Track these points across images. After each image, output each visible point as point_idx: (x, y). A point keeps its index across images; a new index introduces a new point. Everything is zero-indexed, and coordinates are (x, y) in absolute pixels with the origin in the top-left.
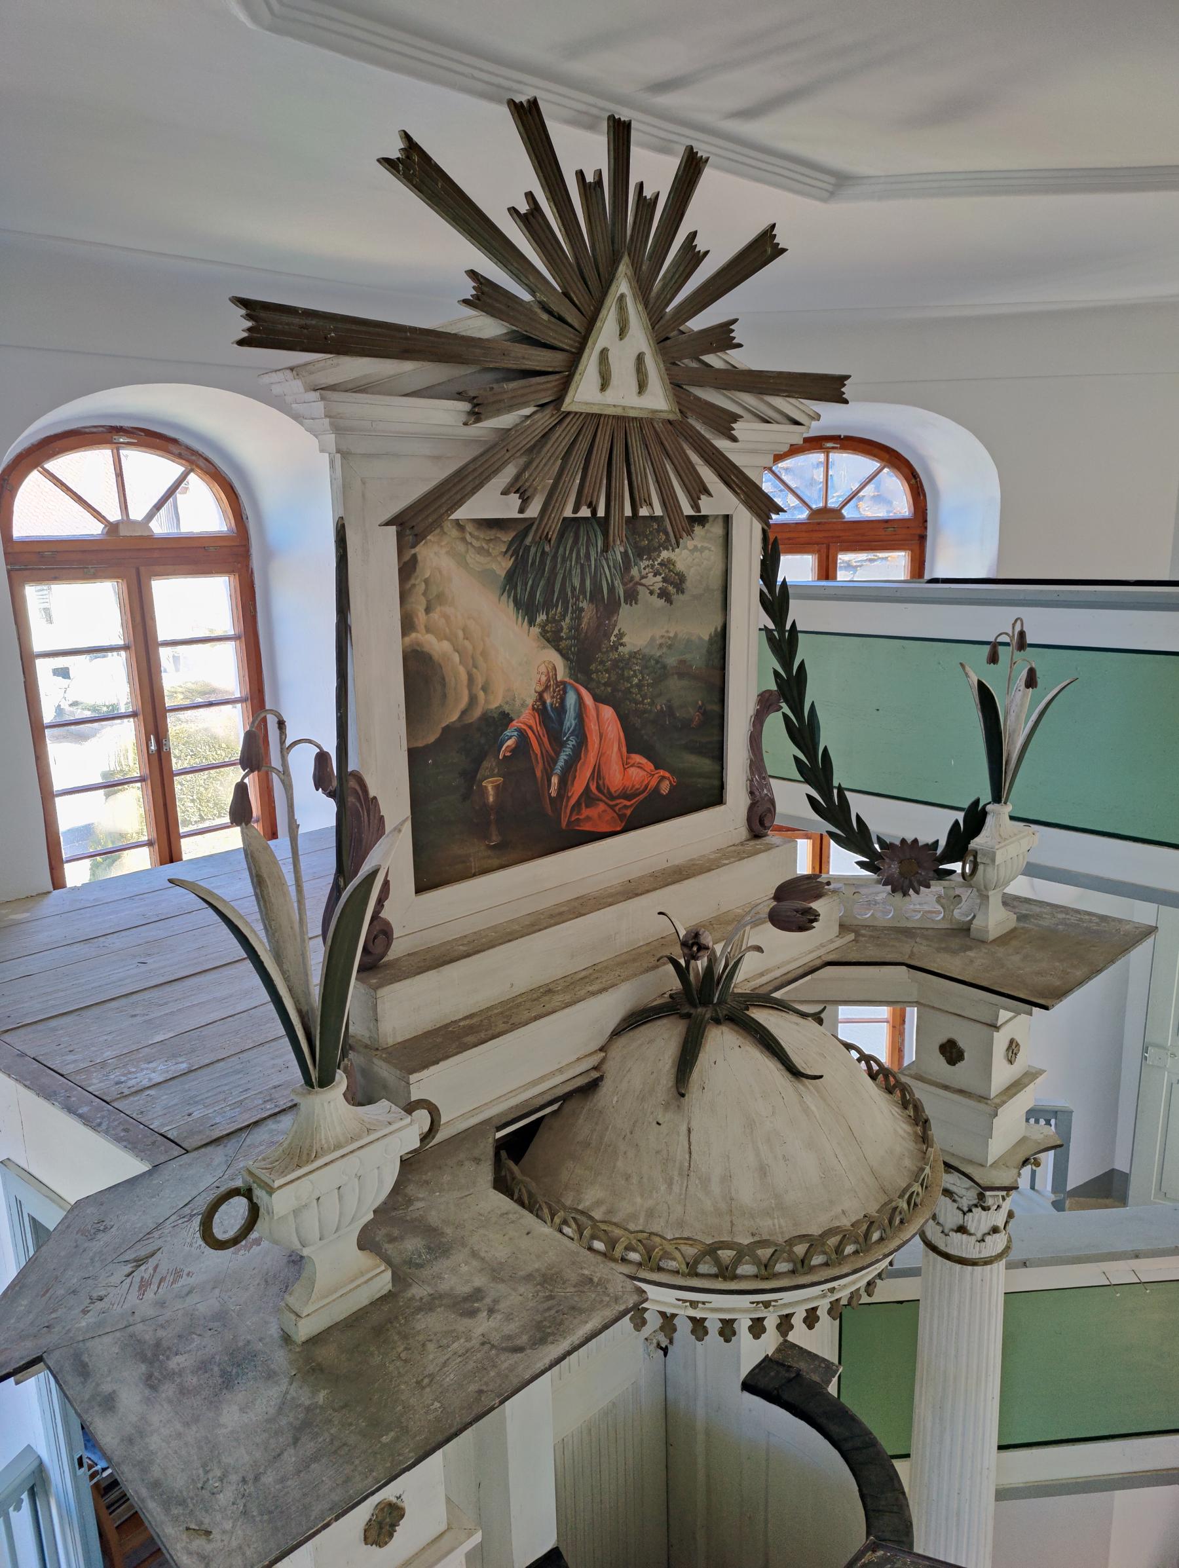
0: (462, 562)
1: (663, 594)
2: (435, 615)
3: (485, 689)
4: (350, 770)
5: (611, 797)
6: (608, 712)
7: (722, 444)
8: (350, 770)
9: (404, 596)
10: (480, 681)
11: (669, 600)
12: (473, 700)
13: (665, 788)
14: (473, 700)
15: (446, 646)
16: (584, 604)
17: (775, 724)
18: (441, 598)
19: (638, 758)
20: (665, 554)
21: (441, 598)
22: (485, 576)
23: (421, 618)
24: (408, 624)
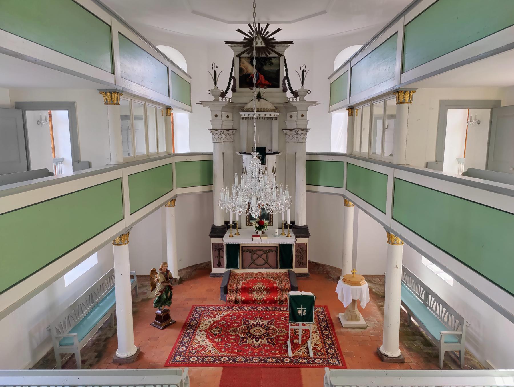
0: (246, 61)
1: (270, 64)
2: (243, 65)
3: (248, 71)
4: (233, 76)
5: (262, 84)
6: (262, 76)
7: (274, 49)
8: (233, 76)
9: (239, 63)
10: (247, 71)
11: (271, 65)
12: (246, 72)
13: (270, 85)
14: (246, 72)
15: (244, 67)
16: (259, 65)
17: (286, 80)
18: (243, 63)
19: (266, 81)
20: (270, 61)
21: (243, 63)
22: (248, 62)
23: (241, 65)
24: (240, 65)
